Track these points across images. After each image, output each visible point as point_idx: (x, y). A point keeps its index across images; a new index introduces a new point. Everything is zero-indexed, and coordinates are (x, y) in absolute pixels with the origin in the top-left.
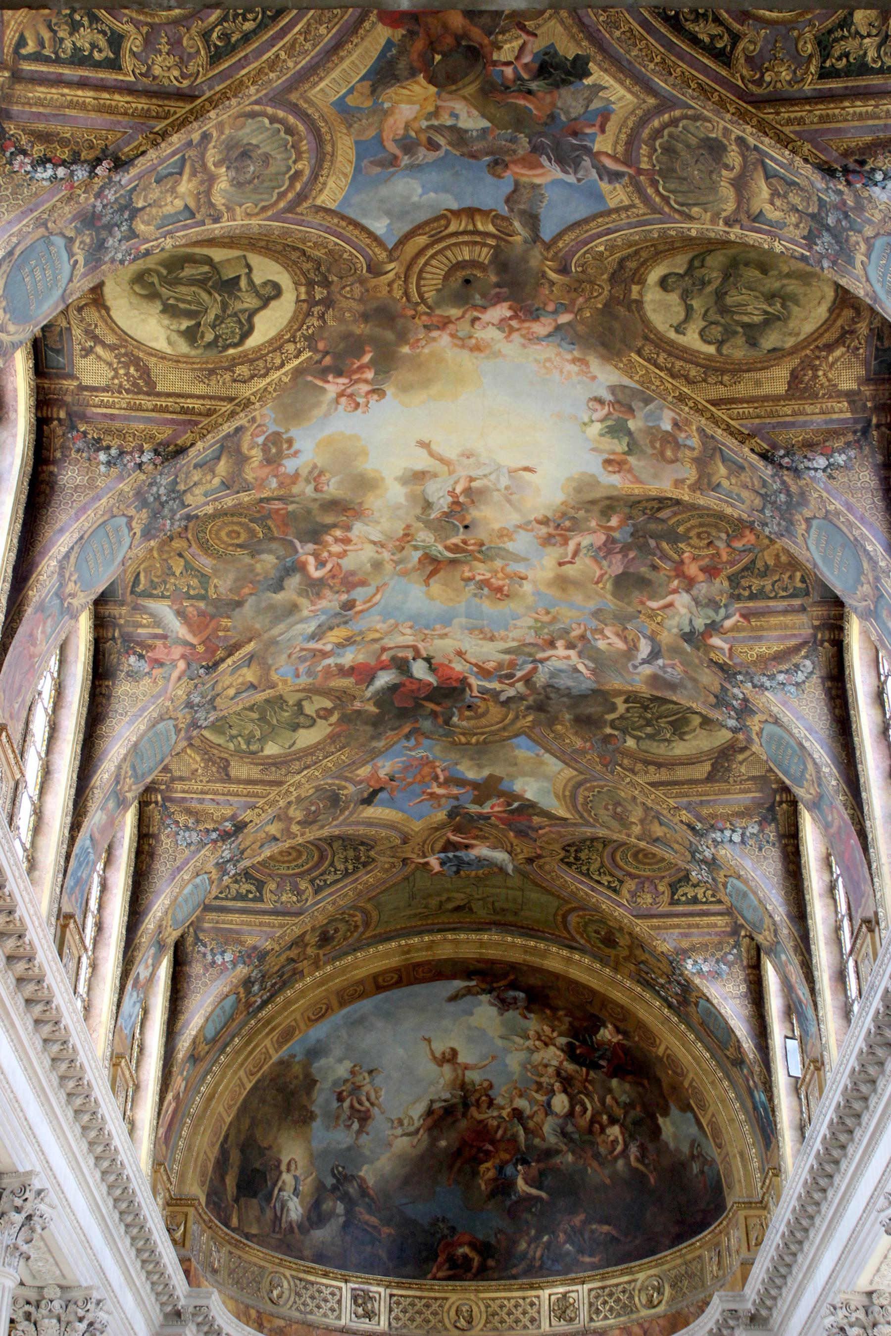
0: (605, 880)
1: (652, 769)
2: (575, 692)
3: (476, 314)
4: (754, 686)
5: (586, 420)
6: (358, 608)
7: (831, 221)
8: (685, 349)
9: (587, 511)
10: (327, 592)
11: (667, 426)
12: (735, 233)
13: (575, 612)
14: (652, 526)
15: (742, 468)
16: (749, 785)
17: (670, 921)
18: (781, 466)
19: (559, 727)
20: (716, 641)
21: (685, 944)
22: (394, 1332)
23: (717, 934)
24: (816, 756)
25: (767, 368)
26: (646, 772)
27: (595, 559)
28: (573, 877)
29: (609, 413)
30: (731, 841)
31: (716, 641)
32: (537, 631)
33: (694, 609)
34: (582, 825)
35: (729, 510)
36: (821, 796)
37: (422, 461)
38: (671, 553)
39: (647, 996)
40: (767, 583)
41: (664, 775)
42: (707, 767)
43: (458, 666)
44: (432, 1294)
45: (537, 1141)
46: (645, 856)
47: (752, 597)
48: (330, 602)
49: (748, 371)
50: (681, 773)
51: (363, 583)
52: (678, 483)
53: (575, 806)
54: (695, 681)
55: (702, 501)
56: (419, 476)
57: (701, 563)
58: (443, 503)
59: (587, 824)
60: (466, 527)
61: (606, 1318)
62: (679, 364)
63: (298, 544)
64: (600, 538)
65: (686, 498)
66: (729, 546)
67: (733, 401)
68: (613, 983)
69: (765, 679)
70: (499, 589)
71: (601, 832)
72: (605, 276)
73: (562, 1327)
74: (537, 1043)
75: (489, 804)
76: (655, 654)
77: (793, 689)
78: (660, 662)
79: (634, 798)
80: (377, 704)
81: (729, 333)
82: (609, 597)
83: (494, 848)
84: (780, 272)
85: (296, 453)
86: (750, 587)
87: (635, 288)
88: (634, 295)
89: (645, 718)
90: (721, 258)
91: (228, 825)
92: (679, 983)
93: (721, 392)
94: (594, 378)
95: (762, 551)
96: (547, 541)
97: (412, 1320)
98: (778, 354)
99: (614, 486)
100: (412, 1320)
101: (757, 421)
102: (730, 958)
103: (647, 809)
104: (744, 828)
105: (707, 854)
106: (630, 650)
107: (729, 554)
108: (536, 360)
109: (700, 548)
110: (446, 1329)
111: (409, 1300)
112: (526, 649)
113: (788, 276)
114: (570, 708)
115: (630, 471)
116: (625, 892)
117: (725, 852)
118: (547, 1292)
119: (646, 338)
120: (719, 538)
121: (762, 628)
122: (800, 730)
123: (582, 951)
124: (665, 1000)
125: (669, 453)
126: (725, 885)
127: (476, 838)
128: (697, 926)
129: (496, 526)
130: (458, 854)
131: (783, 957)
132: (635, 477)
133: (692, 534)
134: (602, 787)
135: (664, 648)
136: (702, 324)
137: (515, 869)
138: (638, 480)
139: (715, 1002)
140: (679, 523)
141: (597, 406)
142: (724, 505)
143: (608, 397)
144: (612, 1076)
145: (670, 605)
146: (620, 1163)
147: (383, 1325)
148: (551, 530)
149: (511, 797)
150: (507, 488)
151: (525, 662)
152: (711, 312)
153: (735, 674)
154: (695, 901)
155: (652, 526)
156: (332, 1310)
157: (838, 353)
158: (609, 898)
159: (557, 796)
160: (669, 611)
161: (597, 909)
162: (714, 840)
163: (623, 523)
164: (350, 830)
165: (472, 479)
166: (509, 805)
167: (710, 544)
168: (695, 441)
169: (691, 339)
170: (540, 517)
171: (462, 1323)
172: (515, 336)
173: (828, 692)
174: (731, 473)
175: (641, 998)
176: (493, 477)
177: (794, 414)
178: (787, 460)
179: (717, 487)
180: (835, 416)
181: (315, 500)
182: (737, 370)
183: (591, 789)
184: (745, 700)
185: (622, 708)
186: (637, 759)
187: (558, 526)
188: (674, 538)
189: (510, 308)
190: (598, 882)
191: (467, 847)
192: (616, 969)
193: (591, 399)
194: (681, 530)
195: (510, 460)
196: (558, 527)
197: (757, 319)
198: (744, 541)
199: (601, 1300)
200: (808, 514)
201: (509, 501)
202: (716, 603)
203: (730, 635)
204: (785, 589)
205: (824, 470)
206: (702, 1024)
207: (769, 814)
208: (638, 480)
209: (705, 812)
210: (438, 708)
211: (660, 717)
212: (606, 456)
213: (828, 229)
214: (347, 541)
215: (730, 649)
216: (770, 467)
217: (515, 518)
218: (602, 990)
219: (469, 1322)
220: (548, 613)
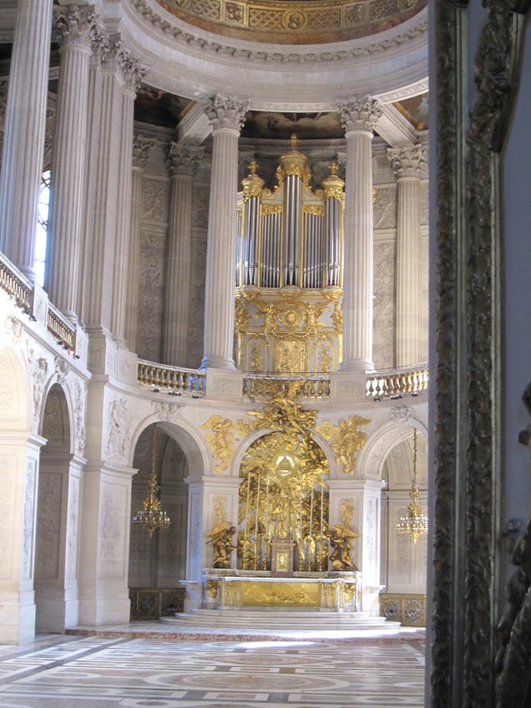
22: (251, 28)
44: (275, 9)
61: (380, 17)
73: (354, 24)
97: (263, 22)
100: (263, 22)
110: (284, 28)
111: (261, 12)
118: (345, 6)
147: (245, 24)
156: (215, 14)
171: (294, 25)
199: (377, 8)
219: (298, 24)
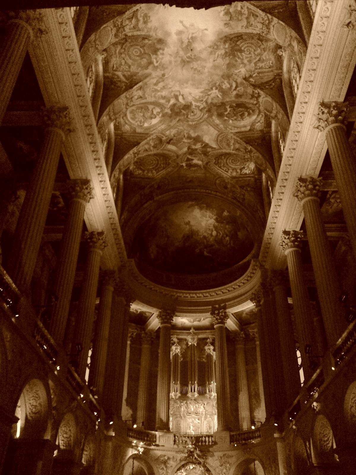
0: (225, 169)
1: (236, 129)
2: (218, 105)
5: (220, 11)
6: (166, 76)
9: (220, 42)
10: (158, 70)
11: (239, 9)
15: (257, 16)
19: (214, 117)
20: (251, 79)
30: (255, 145)
31: (251, 79)
35: (254, 32)
37: (181, 28)
38: (240, 56)
40: (263, 64)
43: (190, 99)
45: (209, 243)
47: (260, 68)
48: (159, 73)
51: (167, 68)
54: (246, 92)
56: (180, 33)
58: (186, 42)
59: (221, 149)
60: (191, 50)
63: (151, 55)
64: (223, 52)
66: (254, 54)
70: (199, 71)
74: (209, 219)
75: (197, 145)
76: (236, 87)
78: (238, 89)
79: (232, 137)
80: (171, 110)
83: (198, 160)
85: (151, 21)
91: (136, 143)
107: (254, 56)
109: (247, 54)
112: (206, 91)
116: (229, 172)
125: (240, 18)
127: (194, 157)
129: (199, 49)
130: (190, 162)
133: (245, 50)
134: (224, 135)
137: (204, 166)
142: (253, 30)
146: (229, 246)
149: (202, 142)
150: (201, 36)
151: (206, 96)
160: (240, 73)
164: (165, 152)
165: (193, 34)
166: (202, 145)
167: (250, 53)
168: (246, 12)
174: (255, 19)
176: (198, 33)
181: (156, 39)
186: (232, 126)
188: (241, 51)
190: (223, 169)
191: (192, 160)
195: (202, 26)
210: (185, 112)
214: (163, 54)
220: (211, 78)
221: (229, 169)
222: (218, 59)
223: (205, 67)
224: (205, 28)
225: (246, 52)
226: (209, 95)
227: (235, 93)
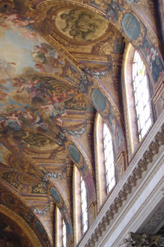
0: (14, 184)
1: (34, 153)
3: (6, 16)
4: (68, 134)
5: (33, 52)
7: (114, 7)
8: (65, 36)
9: (28, 78)
11: (56, 57)
12: (86, 5)
13: (19, 107)
14: (46, 85)
15: (76, 72)
16: (60, 161)
17: (31, 198)
18: (87, 73)
20: (59, 120)
21: (34, 205)
23: (44, 203)
24: (83, 155)
25: (86, 45)
26: (32, 155)
27: (28, 92)
28: (5, 183)
29: (40, 51)
30: (53, 176)
31: (59, 120)
32: (8, 110)
33: (54, 110)
34: (10, 168)
35: (70, 83)
36: (83, 167)
38: (50, 93)
39: (21, 218)
40: (75, 105)
41: (37, 156)
42: (49, 155)
46: (27, 178)
47: (71, 108)
49: (81, 45)
50: (42, 156)
52: (57, 74)
53: (9, 162)
54: (51, 130)
55: (62, 79)
57: (58, 97)
59: (12, 167)
62: (62, 40)
64: (30, 86)
65: (58, 78)
66: (66, 93)
67: (76, 53)
68: (11, 214)
69: (71, 132)
71: (16, 170)
72: (46, 12)
76: (41, 121)
77: (79, 136)
78: (42, 124)
79: (27, 161)
81: (77, 33)
82: (30, 103)
84: (95, 18)
86: (70, 105)
87: (54, 16)
88: (53, 18)
89: (34, 139)
90: (79, 12)
92: (31, 216)
93: (72, 50)
94: (37, 40)
95: (75, 96)
96: (15, 85)
98: (90, 41)
99: (37, 72)
101: (82, 59)
102: (47, 209)
103: (30, 165)
104: (58, 173)
105: (46, 179)
106: (34, 119)
108: (21, 32)
109: (58, 93)
112: (3, 115)
113: (96, 20)
114: (13, 134)
115: (43, 68)
117: (51, 179)
119: (54, 31)
120: (64, 91)
121: (72, 118)
122: (80, 148)
123: (4, 204)
124: (26, 220)
125: (55, 65)
126: (50, 189)
128: (38, 200)
131: (65, 211)
132: (44, 70)
133: (57, 88)
135: (44, 119)
136: (71, 30)
138: (45, 71)
139: (41, 222)
140: (53, 85)
141: (37, 48)
143: (40, 46)
144: (7, 241)
145: (47, 108)
148: (17, 82)
150: (6, 68)
151: (2, 119)
152: (74, 26)
153: (63, 130)
154: (39, 192)
155: (46, 85)
157: (107, 43)
158: (14, 189)
159: (4, 158)
160: (47, 110)
161: (10, 192)
162: (49, 176)
163: (38, 83)
168: (64, 63)
169: (67, 34)
170: (14, 78)
172: (17, 24)
173: (88, 137)
174: (72, 73)
175: (19, 219)
176: (2, 64)
177: (92, 59)
178: (88, 72)
179: (67, 76)
180: (103, 61)
182: (78, 44)
183: (14, 158)
184: (65, 137)
185: (28, 135)
186: (30, 150)
187: (19, 81)
188: (51, 89)
189: (17, 16)
190: (12, 185)
192: (13, 210)
193: (35, 46)
194: (54, 87)
196: (19, 81)
197: (86, 31)
198: (71, 92)
200: (92, 87)
201: (6, 72)
202: (60, 109)
203: (63, 118)
204: (80, 107)
205: (99, 76)
206: (36, 228)
207: (65, 171)
208: (45, 71)
209: (47, 167)
211: (38, 139)
212: (37, 63)
213: (113, 9)
215: (63, 122)
216: (84, 73)
217: (7, 77)
218: (8, 216)
220: (12, 105)
221: (18, 185)
222: (23, 91)
223: (6, 95)
224: (13, 62)
225: (57, 91)
226: (5, 119)
227: (38, 125)
